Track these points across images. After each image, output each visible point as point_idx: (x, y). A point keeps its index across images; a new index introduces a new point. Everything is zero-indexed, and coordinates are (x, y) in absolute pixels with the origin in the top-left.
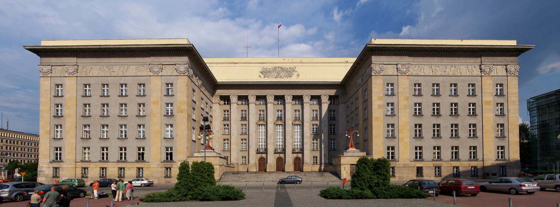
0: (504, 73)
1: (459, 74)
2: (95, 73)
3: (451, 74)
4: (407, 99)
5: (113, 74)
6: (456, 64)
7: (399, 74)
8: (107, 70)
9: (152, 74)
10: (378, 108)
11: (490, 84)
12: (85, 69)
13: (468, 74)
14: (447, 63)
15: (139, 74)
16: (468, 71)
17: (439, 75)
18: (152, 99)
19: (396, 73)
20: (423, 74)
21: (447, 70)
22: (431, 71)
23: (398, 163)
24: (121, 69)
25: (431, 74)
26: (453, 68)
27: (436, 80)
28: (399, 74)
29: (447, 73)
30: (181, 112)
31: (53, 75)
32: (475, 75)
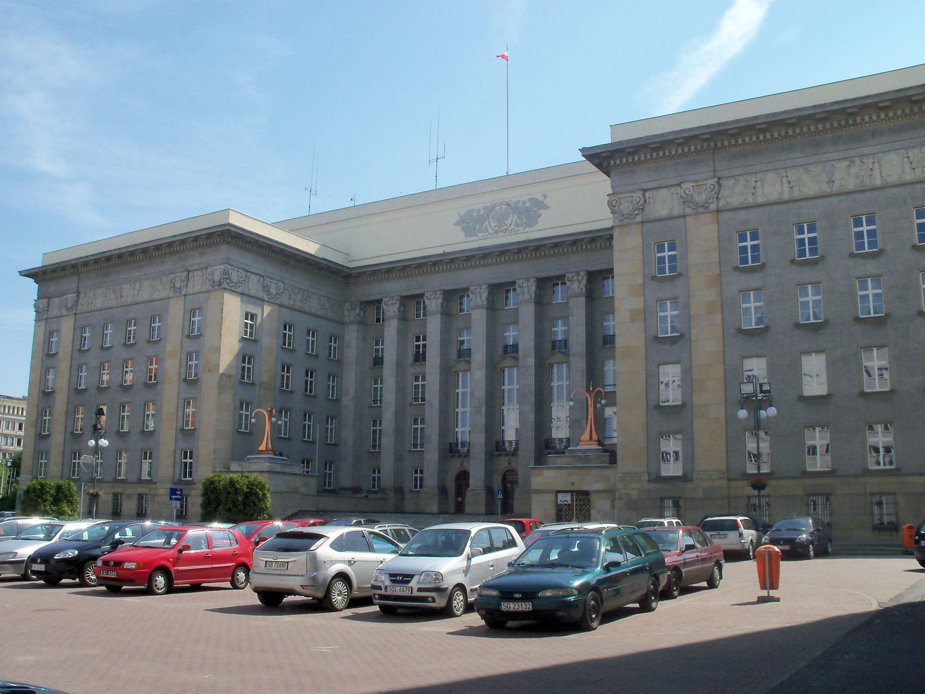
1: (878, 182)
2: (98, 304)
6: (866, 151)
7: (689, 211)
13: (908, 177)
14: (835, 155)
15: (155, 297)
20: (760, 200)
21: (837, 176)
22: (786, 187)
23: (690, 485)
25: (786, 196)
26: (854, 170)
28: (689, 211)
30: (210, 371)
31: (50, 314)
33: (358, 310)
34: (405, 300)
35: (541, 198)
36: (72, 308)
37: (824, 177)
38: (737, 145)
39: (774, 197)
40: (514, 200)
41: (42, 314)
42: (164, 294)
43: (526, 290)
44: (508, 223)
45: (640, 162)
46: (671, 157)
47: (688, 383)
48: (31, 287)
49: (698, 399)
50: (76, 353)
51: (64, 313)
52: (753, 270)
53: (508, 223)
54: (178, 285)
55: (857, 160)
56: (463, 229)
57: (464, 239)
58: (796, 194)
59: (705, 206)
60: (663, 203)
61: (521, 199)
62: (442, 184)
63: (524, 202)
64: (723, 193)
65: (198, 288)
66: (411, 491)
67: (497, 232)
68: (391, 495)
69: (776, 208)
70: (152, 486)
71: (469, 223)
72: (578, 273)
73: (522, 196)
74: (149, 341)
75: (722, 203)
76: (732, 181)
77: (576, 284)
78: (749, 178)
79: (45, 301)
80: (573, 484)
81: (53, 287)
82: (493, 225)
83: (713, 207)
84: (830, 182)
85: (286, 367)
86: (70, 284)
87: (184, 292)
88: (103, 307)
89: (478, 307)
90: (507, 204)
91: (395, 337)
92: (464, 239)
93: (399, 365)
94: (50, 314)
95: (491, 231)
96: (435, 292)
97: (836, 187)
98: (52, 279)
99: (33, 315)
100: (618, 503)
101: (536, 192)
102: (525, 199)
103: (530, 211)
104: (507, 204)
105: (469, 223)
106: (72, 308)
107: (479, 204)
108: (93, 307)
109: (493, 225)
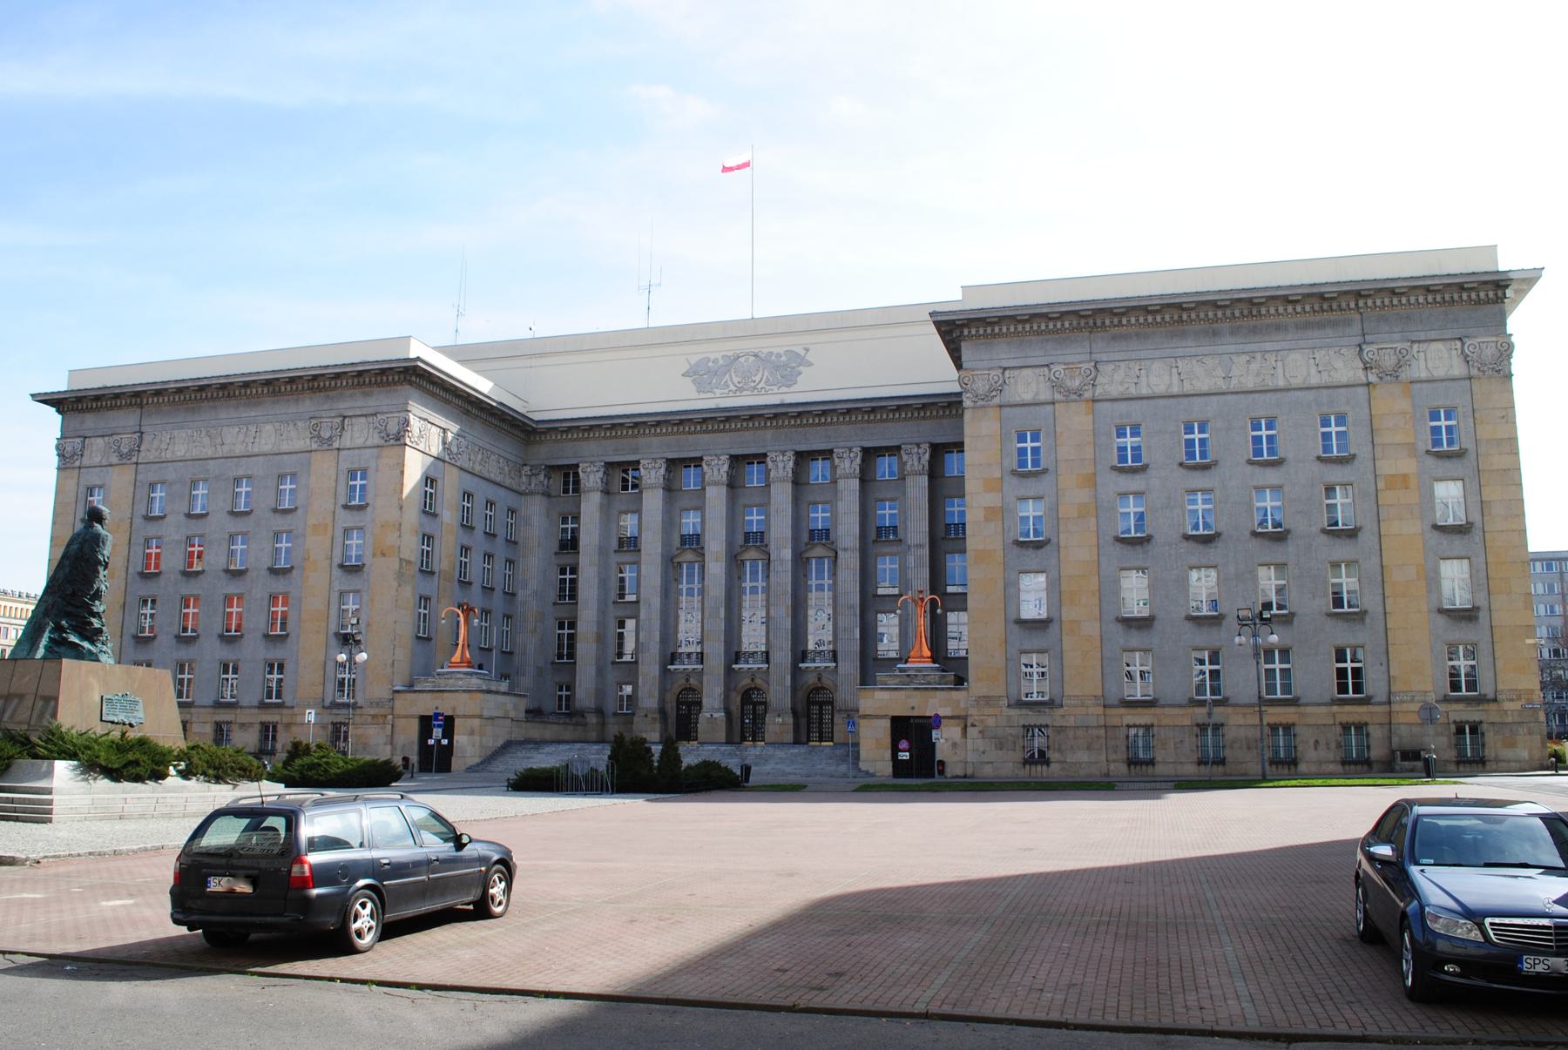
0: (1458, 369)
1: (1281, 383)
2: (180, 451)
3: (1250, 385)
4: (1091, 481)
5: (221, 452)
6: (1268, 346)
7: (1058, 397)
8: (206, 440)
9: (314, 446)
10: (987, 519)
11: (1404, 413)
12: (156, 443)
14: (1232, 348)
15: (285, 447)
16: (1313, 370)
17: (1205, 388)
18: (312, 521)
19: (1045, 395)
20: (1145, 391)
21: (1235, 372)
22: (1175, 378)
24: (241, 437)
25: (1175, 390)
26: (1254, 366)
27: (1197, 409)
29: (1234, 382)
31: (86, 461)
32: (1344, 380)
33: (542, 477)
35: (802, 353)
36: (129, 454)
37: (1220, 372)
38: (1120, 324)
39: (1161, 389)
41: (68, 459)
42: (303, 443)
43: (781, 465)
44: (757, 379)
45: (1000, 335)
46: (1039, 333)
47: (1055, 590)
48: (52, 419)
49: (1067, 614)
50: (138, 521)
51: (115, 460)
52: (1133, 471)
54: (326, 434)
55: (1258, 356)
56: (694, 381)
57: (696, 395)
58: (1187, 388)
59: (1078, 393)
60: (1027, 386)
61: (775, 351)
62: (656, 322)
63: (778, 355)
64: (1100, 379)
65: (359, 442)
66: (615, 714)
67: (741, 389)
68: (592, 719)
69: (1162, 402)
70: (285, 711)
71: (700, 374)
72: (850, 450)
73: (778, 346)
74: (275, 511)
75: (1099, 391)
76: (1111, 366)
78: (1132, 364)
79: (78, 440)
81: (90, 421)
82: (736, 380)
83: (1088, 395)
84: (1227, 378)
85: (465, 550)
86: (127, 419)
87: (336, 445)
88: (188, 456)
89: (716, 484)
91: (597, 515)
92: (696, 395)
93: (602, 551)
94: (86, 461)
97: (1234, 384)
98: (89, 410)
99: (55, 460)
100: (972, 732)
101: (796, 344)
103: (788, 367)
105: (700, 374)
106: (129, 454)
107: (716, 352)
108: (169, 456)
109: (736, 380)
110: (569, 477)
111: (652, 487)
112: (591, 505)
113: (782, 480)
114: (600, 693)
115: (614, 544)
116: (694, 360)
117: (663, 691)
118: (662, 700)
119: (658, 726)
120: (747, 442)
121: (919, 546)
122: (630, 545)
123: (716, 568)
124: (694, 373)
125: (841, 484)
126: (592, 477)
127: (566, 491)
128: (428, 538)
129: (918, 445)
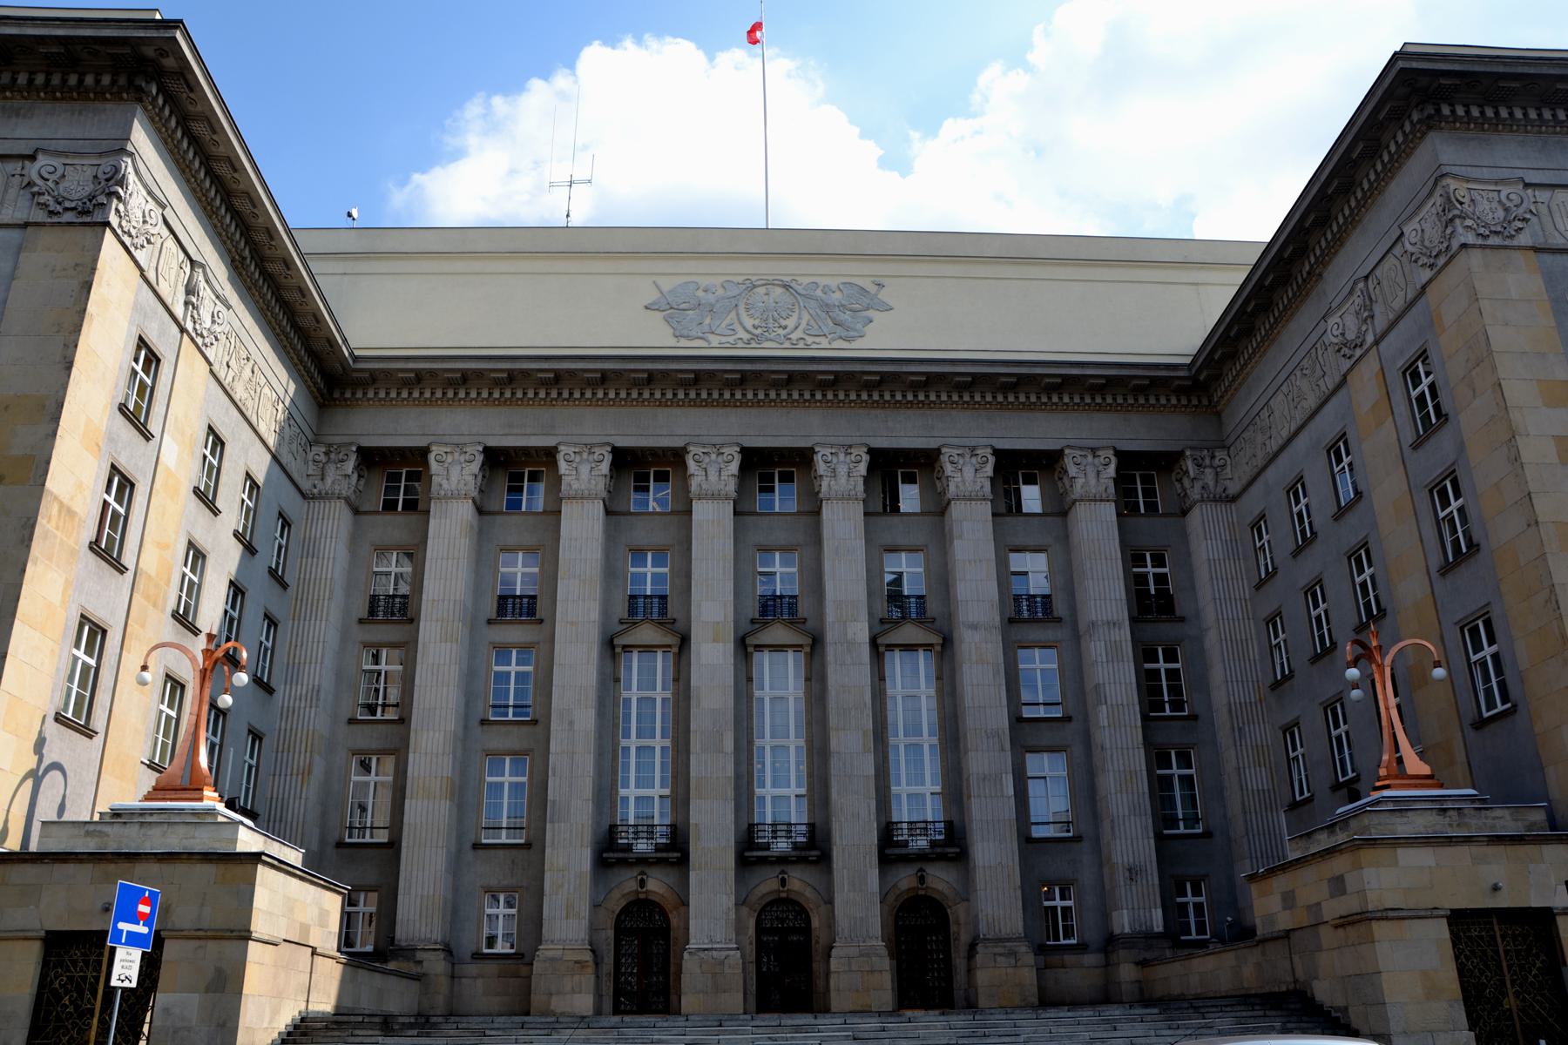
34: (497, 461)
35: (872, 289)
40: (806, 281)
43: (842, 470)
44: (791, 323)
53: (791, 323)
61: (823, 281)
63: (826, 290)
66: (478, 956)
73: (827, 276)
77: (969, 472)
80: (1496, 888)
85: (197, 556)
89: (714, 497)
90: (786, 287)
92: (672, 342)
95: (746, 336)
96: (590, 447)
101: (862, 274)
102: (833, 283)
104: (786, 287)
107: (712, 277)
109: (749, 323)
110: (397, 476)
111: (580, 497)
112: (450, 525)
113: (846, 498)
114: (454, 912)
115: (490, 608)
116: (667, 284)
117: (596, 906)
118: (593, 929)
119: (588, 979)
120: (777, 428)
121: (1112, 624)
122: (520, 608)
123: (712, 655)
124: (669, 308)
125: (957, 510)
126: (455, 472)
127: (390, 506)
128: (122, 483)
129: (1093, 450)
